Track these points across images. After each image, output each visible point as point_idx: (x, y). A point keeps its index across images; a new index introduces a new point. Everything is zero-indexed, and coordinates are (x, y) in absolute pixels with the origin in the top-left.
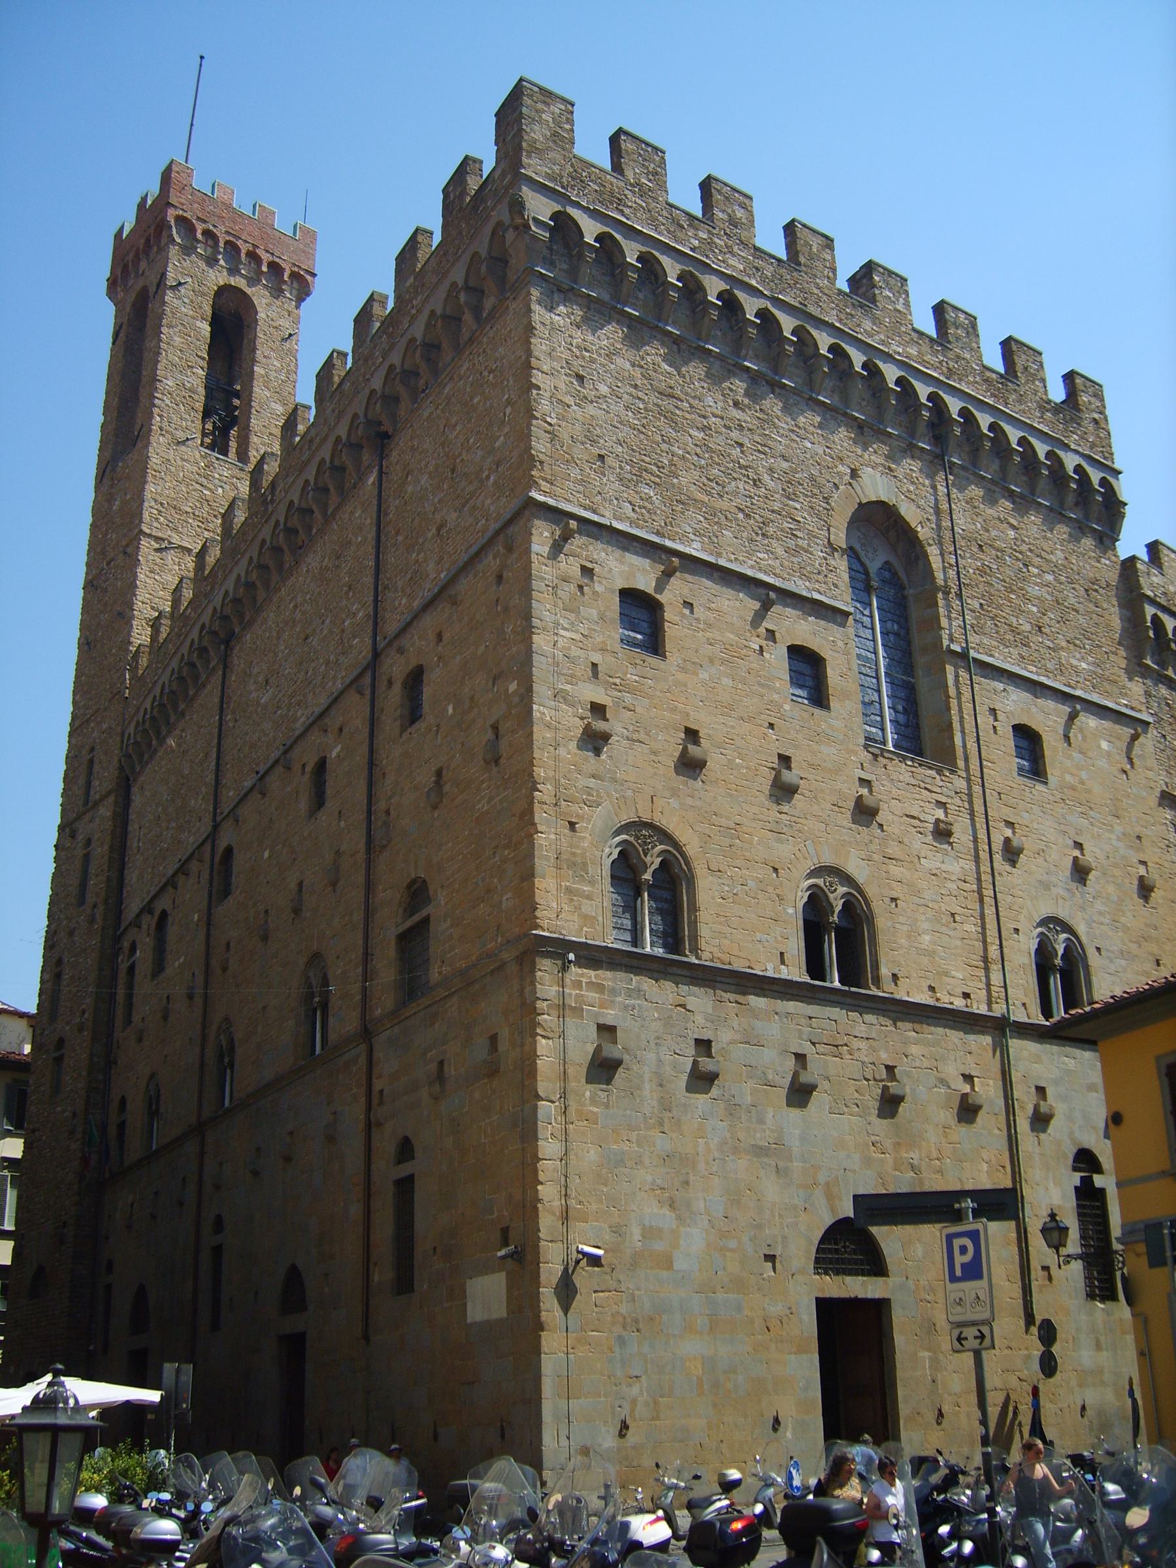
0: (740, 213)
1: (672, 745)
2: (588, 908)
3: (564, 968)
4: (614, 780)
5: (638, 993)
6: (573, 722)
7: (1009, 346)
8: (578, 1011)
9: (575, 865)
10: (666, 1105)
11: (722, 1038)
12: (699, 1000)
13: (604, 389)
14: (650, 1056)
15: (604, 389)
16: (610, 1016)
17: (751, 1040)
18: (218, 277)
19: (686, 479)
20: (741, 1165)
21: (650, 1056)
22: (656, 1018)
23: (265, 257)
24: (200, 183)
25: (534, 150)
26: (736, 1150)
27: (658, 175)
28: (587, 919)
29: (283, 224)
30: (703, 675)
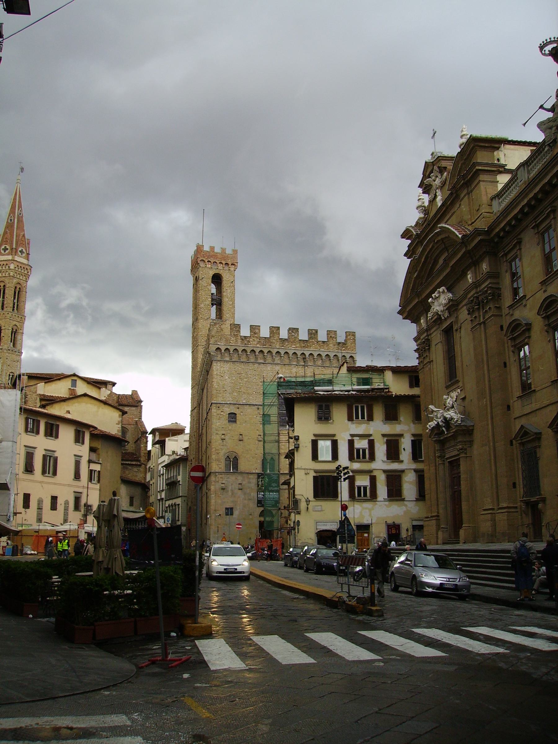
0: (257, 331)
1: (237, 438)
2: (220, 466)
3: (216, 476)
4: (226, 445)
5: (229, 478)
6: (218, 437)
7: (329, 332)
8: (218, 482)
9: (218, 460)
10: (232, 494)
11: (244, 483)
12: (240, 479)
13: (227, 378)
14: (230, 488)
15: (227, 378)
16: (224, 482)
17: (250, 483)
18: (211, 273)
19: (242, 390)
20: (246, 502)
21: (230, 488)
22: (232, 481)
23: (224, 262)
24: (206, 248)
25: (213, 336)
26: (245, 499)
27: (239, 331)
28: (220, 468)
29: (229, 251)
30: (244, 424)
